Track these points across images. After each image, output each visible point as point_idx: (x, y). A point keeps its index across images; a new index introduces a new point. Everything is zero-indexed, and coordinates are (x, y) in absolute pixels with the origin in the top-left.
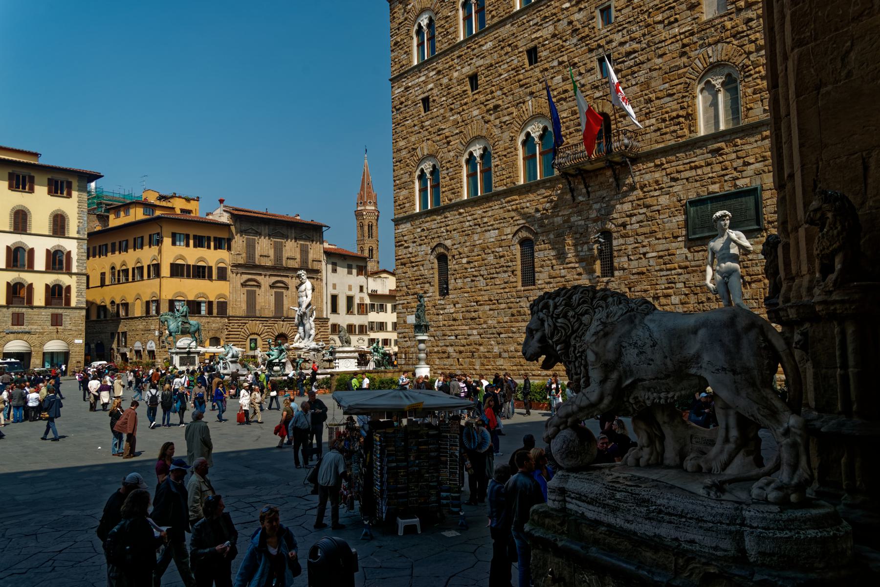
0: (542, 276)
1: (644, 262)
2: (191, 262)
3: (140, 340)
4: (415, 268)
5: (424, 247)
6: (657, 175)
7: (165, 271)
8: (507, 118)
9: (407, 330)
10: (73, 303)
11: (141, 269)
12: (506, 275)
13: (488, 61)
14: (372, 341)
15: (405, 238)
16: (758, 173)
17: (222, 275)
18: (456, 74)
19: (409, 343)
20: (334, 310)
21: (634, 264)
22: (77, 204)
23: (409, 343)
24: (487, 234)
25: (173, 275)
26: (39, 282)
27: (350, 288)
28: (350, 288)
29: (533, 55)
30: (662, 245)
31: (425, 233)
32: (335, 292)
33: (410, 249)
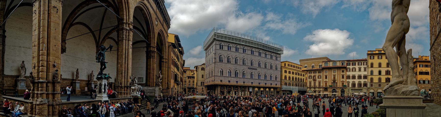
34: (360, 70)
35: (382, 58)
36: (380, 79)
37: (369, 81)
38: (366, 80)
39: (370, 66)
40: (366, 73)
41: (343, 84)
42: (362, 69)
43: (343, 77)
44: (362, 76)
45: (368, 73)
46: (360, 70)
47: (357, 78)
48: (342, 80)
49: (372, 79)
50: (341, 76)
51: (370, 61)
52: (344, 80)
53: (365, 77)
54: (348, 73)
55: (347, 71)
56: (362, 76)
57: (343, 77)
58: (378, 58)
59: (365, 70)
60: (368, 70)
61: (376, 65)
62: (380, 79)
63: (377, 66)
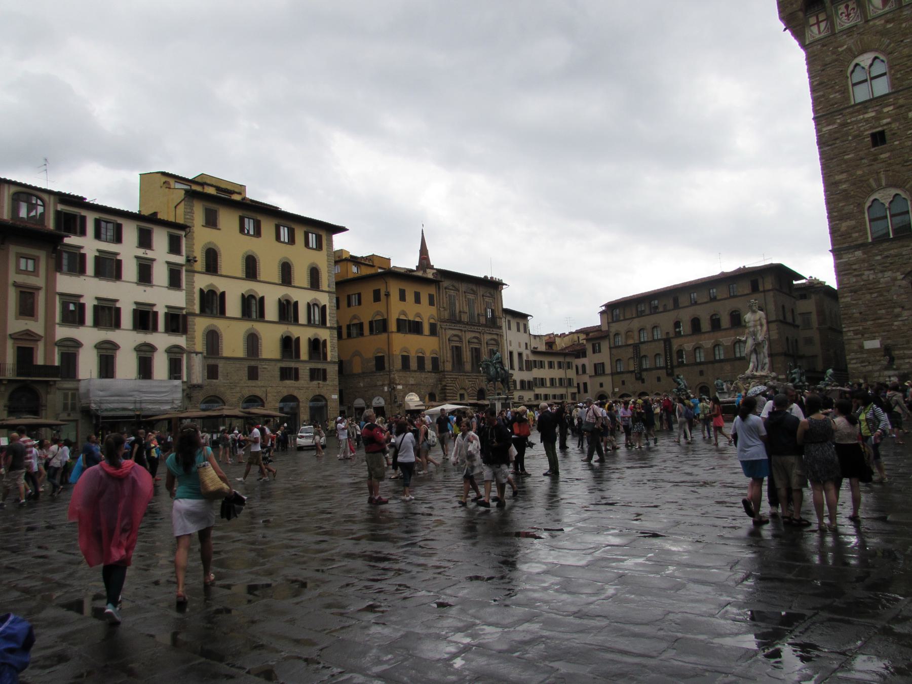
2: (411, 318)
3: (363, 397)
4: (875, 295)
5: (888, 274)
7: (393, 326)
9: (865, 356)
10: (329, 359)
11: (361, 326)
14: (537, 397)
15: (854, 267)
17: (433, 331)
19: (870, 368)
20: (512, 367)
22: (326, 258)
23: (870, 368)
25: (399, 330)
26: (303, 334)
27: (520, 346)
28: (520, 346)
31: (889, 260)
32: (510, 349)
33: (865, 277)
34: (145, 274)
35: (258, 233)
36: (253, 341)
37: (200, 345)
38: (180, 340)
39: (200, 265)
40: (178, 299)
41: (25, 355)
42: (160, 274)
43: (27, 308)
44: (161, 311)
45: (189, 300)
46: (145, 274)
47: (127, 319)
48: (16, 325)
49: (213, 338)
50: (12, 297)
51: (202, 236)
52: (37, 326)
53: (177, 322)
54: (66, 283)
55: (59, 268)
56: (161, 311)
57: (27, 308)
58: (242, 230)
59: (175, 281)
60: (191, 283)
61: (231, 262)
62: (253, 341)
63: (239, 269)
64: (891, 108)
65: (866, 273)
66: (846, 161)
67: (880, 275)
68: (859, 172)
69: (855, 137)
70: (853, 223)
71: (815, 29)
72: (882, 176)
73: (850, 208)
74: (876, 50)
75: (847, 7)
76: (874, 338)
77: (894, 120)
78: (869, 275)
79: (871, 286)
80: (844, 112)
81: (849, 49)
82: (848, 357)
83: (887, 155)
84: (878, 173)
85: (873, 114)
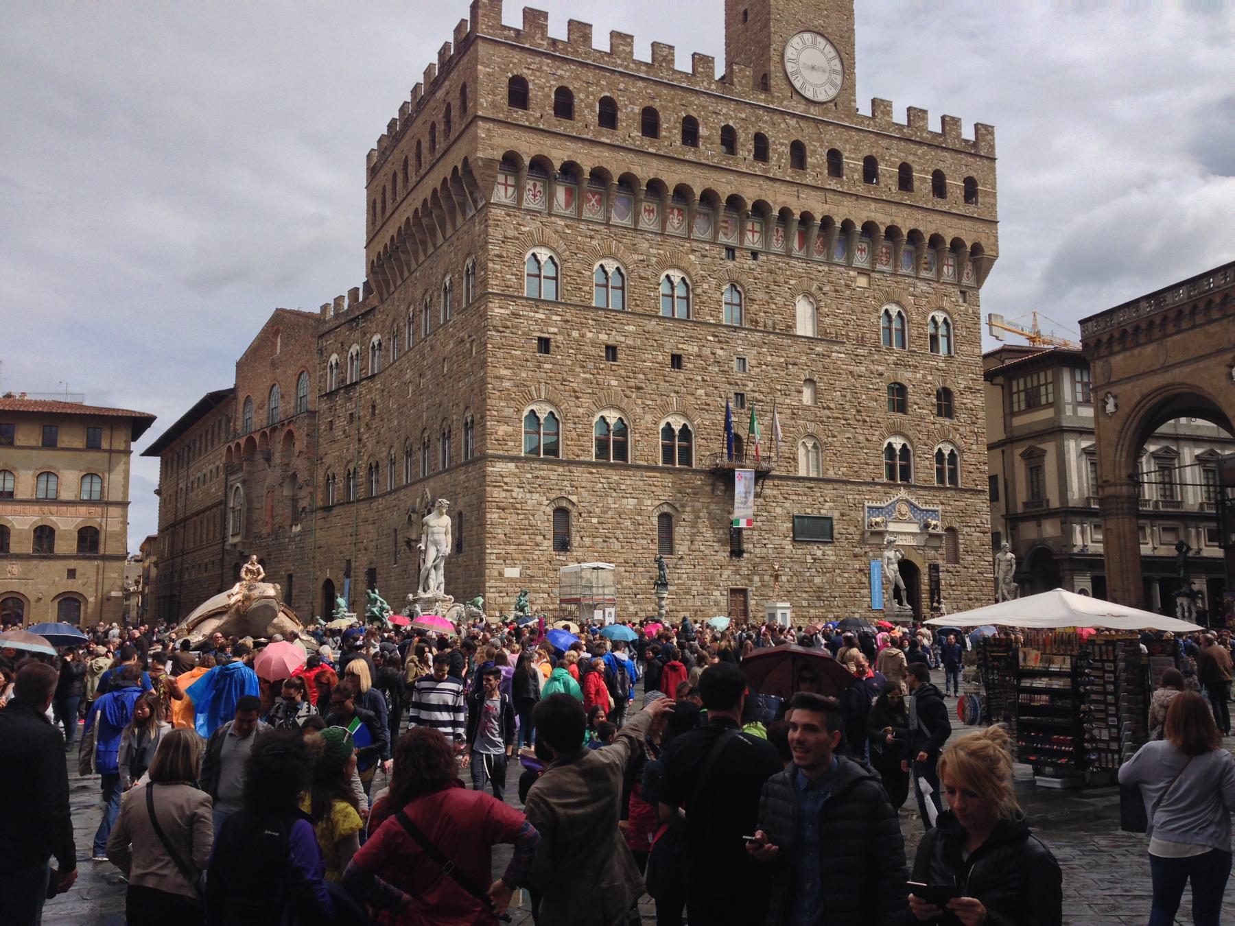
0: (682, 548)
1: (765, 550)
4: (521, 517)
5: (536, 496)
6: (775, 492)
8: (649, 402)
12: (645, 542)
13: (630, 342)
16: (831, 508)
18: (589, 335)
19: (507, 599)
21: (758, 550)
23: (507, 599)
24: (624, 501)
29: (677, 361)
30: (777, 541)
64: (559, 318)
65: (516, 489)
66: (512, 357)
67: (528, 496)
68: (524, 375)
69: (524, 334)
70: (510, 429)
71: (502, 189)
72: (543, 387)
73: (509, 412)
74: (553, 250)
75: (535, 186)
76: (514, 565)
77: (560, 333)
78: (518, 493)
79: (519, 506)
80: (519, 301)
81: (530, 233)
82: (488, 584)
83: (550, 366)
84: (539, 383)
85: (543, 317)
